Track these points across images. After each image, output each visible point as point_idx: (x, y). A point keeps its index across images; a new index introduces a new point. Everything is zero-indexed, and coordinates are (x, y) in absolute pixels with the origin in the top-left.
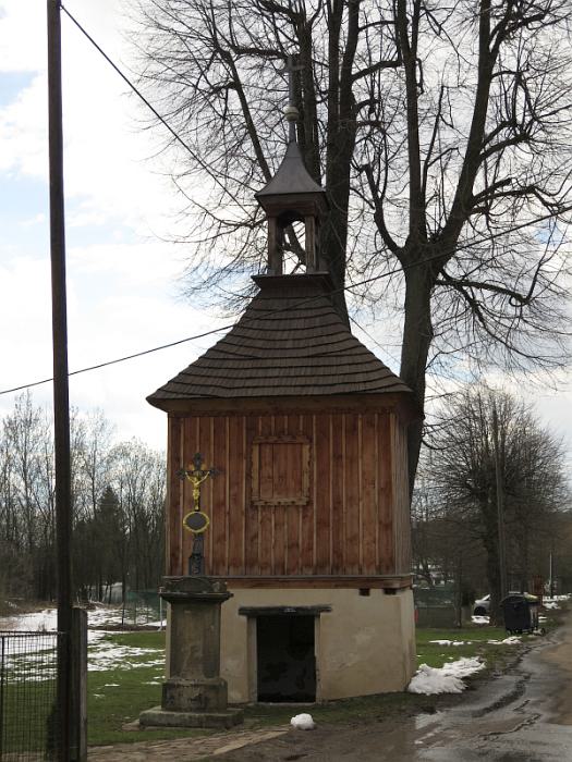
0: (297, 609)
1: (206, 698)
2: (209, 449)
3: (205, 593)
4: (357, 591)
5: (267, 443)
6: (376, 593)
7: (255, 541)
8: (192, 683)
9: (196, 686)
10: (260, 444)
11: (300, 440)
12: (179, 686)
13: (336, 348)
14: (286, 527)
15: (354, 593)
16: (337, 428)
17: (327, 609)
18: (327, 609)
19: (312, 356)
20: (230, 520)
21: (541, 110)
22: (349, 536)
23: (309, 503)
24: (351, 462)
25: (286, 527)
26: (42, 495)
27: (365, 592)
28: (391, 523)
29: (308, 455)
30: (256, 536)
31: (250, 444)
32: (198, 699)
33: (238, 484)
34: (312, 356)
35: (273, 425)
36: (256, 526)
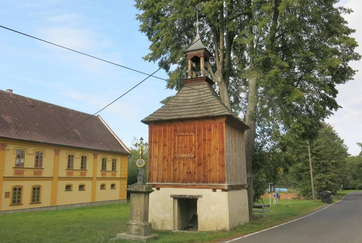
0: (191, 196)
1: (140, 230)
2: (161, 138)
3: (140, 189)
4: (211, 190)
5: (180, 136)
6: (219, 191)
7: (176, 171)
8: (135, 224)
9: (137, 225)
10: (178, 136)
11: (192, 134)
12: (131, 225)
13: (206, 101)
14: (187, 165)
15: (210, 191)
16: (205, 129)
17: (201, 196)
18: (201, 196)
19: (198, 104)
20: (168, 163)
21: (191, 8)
22: (209, 169)
23: (195, 157)
24: (165, 137)
25: (187, 165)
26: (122, 158)
27: (214, 190)
28: (224, 164)
29: (194, 139)
30: (176, 169)
31: (175, 136)
32: (137, 230)
33: (171, 150)
34: (198, 104)
35: (182, 129)
36: (177, 166)
